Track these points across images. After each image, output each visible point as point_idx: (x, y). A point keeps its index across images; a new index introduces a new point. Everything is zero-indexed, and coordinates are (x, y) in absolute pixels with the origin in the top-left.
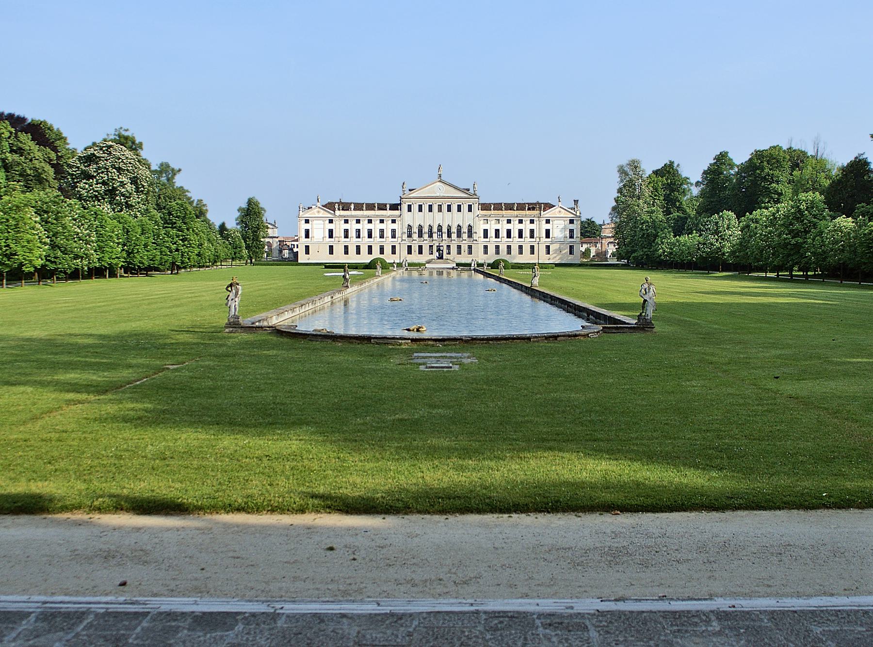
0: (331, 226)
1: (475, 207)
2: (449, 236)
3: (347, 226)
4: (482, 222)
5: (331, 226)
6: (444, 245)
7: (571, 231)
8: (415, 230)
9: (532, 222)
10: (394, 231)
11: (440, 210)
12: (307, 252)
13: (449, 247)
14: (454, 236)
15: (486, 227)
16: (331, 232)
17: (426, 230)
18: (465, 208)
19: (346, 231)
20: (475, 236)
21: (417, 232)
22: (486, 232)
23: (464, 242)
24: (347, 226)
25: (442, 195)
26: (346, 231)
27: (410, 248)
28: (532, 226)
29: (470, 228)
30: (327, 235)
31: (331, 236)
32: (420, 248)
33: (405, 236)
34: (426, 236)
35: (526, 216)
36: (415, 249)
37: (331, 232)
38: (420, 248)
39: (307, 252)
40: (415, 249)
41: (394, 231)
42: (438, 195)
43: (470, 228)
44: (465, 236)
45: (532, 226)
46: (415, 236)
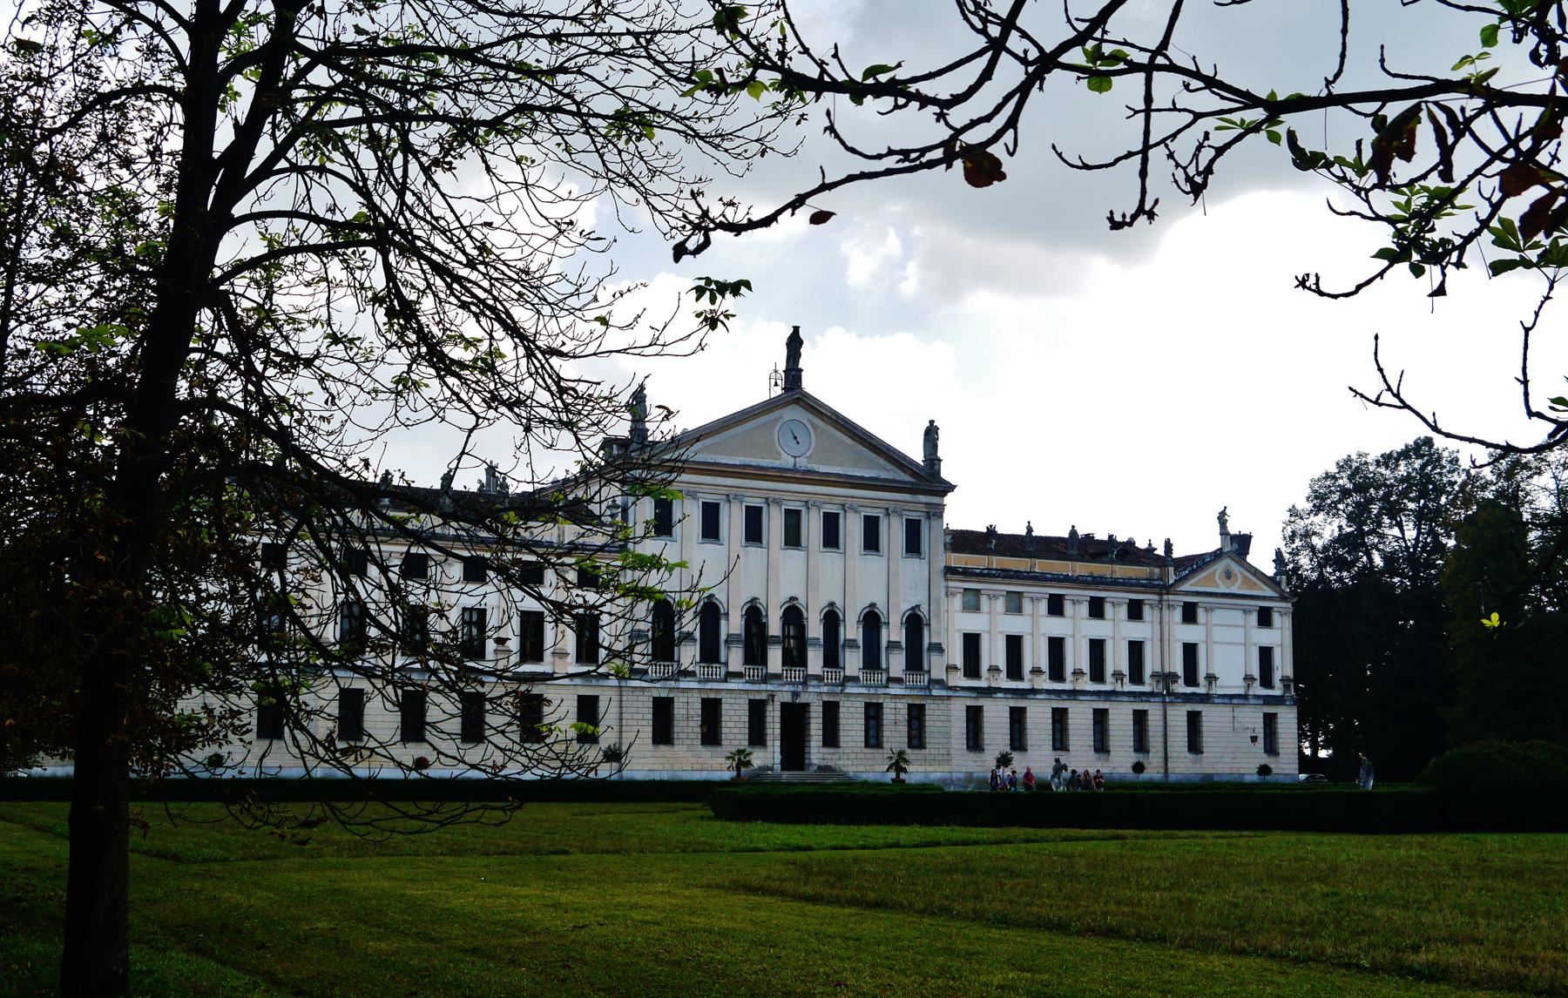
1: (931, 539)
2: (832, 659)
4: (957, 602)
6: (814, 698)
7: (1266, 654)
9: (1135, 612)
13: (831, 712)
14: (853, 662)
15: (973, 622)
18: (893, 534)
20: (936, 666)
21: (697, 635)
22: (972, 642)
23: (895, 690)
25: (803, 463)
27: (663, 712)
28: (1137, 631)
29: (915, 623)
32: (711, 711)
34: (735, 658)
35: (1114, 583)
36: (687, 712)
38: (711, 711)
40: (687, 712)
42: (786, 461)
43: (915, 623)
44: (896, 663)
45: (1137, 631)
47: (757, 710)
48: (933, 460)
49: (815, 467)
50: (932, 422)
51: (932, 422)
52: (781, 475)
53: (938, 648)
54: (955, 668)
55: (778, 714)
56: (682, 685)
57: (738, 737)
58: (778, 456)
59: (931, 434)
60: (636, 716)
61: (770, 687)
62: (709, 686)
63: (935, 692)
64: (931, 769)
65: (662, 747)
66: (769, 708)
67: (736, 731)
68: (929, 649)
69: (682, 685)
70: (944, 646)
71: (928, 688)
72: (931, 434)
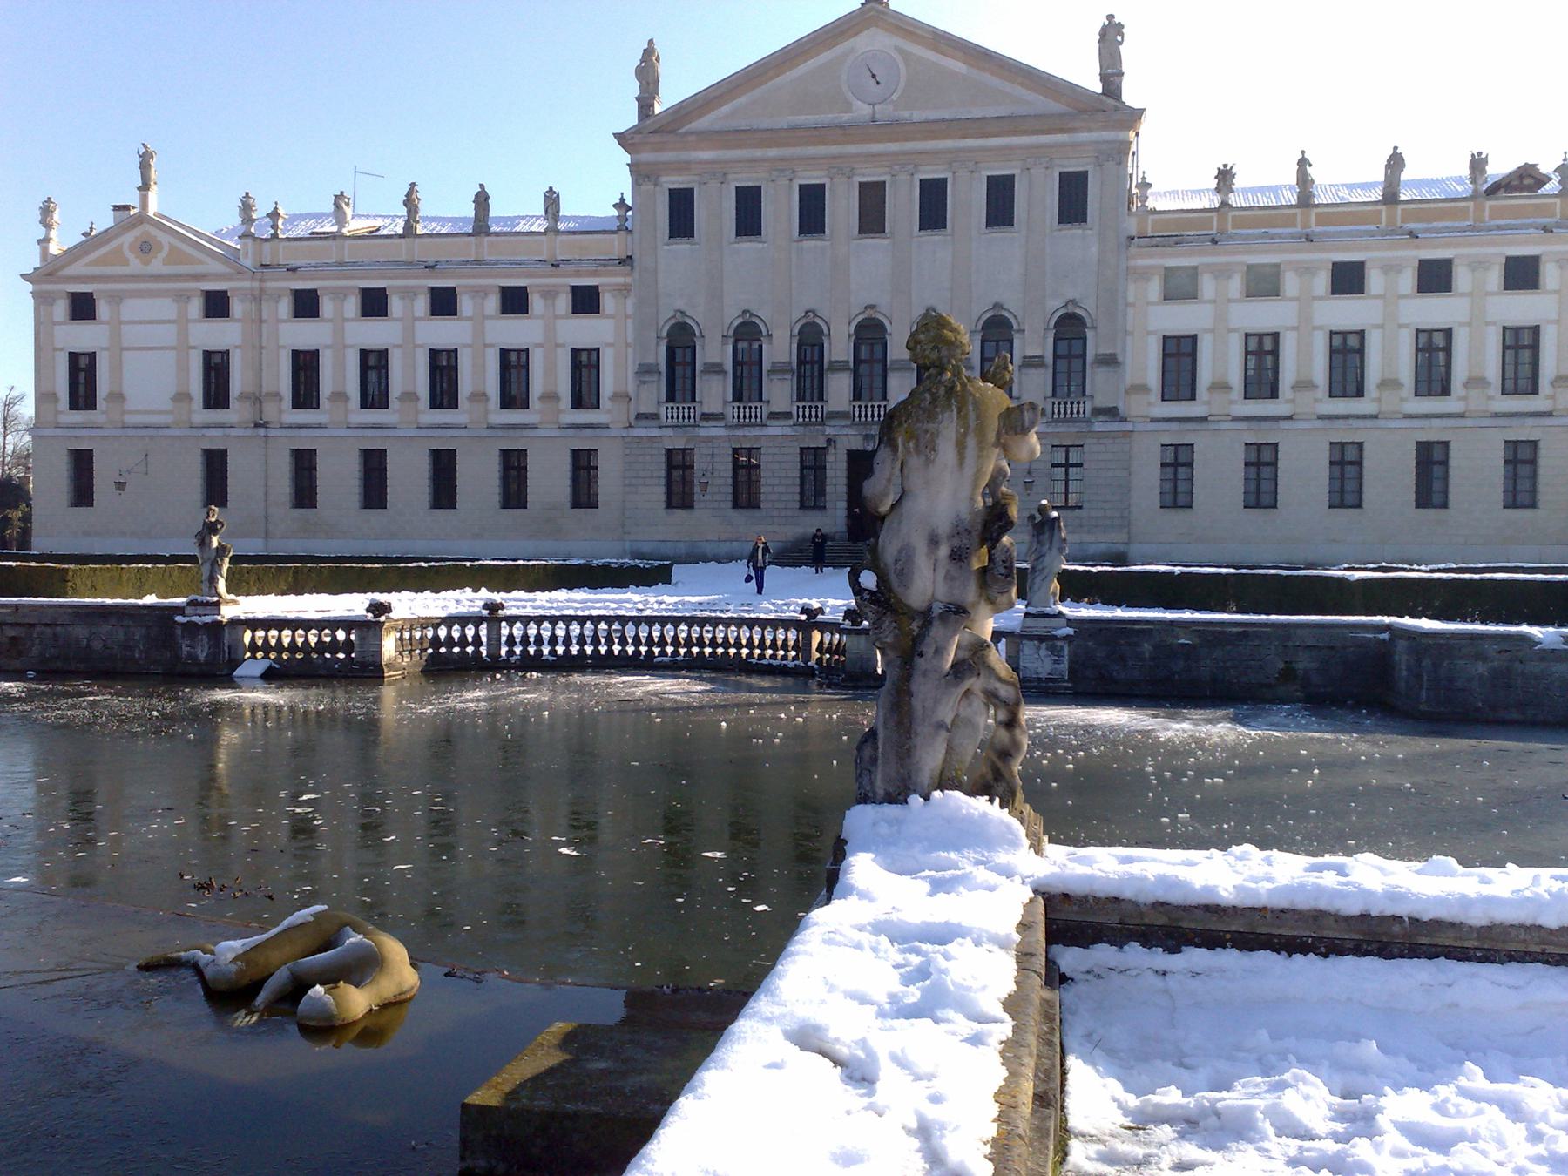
0: (220, 334)
3: (306, 334)
5: (220, 334)
8: (714, 350)
10: (584, 364)
11: (872, 218)
12: (83, 494)
16: (216, 369)
17: (780, 348)
19: (305, 365)
20: (1101, 386)
21: (729, 366)
24: (306, 334)
25: (884, 112)
26: (305, 365)
28: (1521, 308)
29: (1070, 328)
30: (196, 387)
31: (216, 391)
33: (652, 396)
34: (779, 393)
36: (713, 468)
37: (216, 369)
39: (83, 494)
40: (713, 468)
41: (584, 364)
42: (862, 110)
43: (1070, 328)
46: (714, 393)
47: (812, 463)
48: (1111, 77)
49: (905, 114)
50: (1110, 17)
51: (1110, 17)
52: (849, 132)
53: (1110, 361)
54: (1143, 389)
55: (844, 465)
56: (702, 432)
57: (784, 498)
58: (848, 107)
59: (1111, 35)
60: (642, 474)
61: (829, 431)
62: (739, 432)
63: (1098, 427)
64: (1092, 538)
65: (680, 513)
66: (830, 458)
67: (781, 489)
68: (1092, 364)
69: (702, 432)
70: (1120, 358)
71: (1089, 422)
72: (1111, 35)
